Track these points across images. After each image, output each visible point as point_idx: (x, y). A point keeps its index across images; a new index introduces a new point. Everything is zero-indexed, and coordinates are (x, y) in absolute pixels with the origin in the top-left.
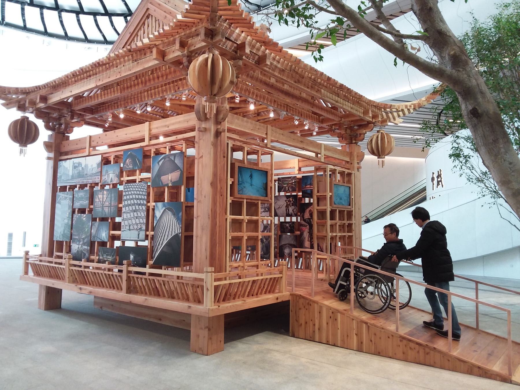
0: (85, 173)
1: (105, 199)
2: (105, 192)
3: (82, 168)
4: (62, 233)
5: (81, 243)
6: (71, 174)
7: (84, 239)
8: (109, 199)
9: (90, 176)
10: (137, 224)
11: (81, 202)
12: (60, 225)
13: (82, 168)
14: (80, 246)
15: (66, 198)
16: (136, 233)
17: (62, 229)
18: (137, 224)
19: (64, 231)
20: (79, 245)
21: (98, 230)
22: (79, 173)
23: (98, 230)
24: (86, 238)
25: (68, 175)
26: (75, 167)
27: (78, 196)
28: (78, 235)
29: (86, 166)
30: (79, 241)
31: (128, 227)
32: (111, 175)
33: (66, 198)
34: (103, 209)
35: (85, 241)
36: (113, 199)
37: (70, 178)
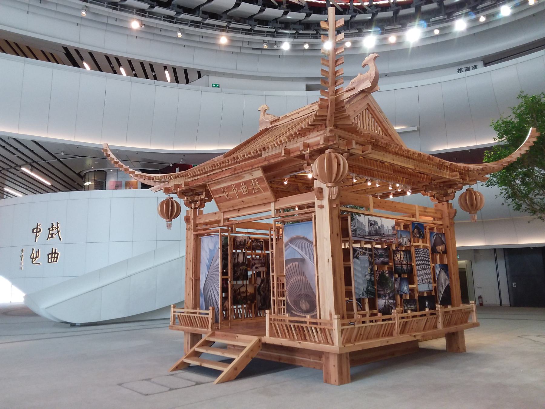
0: (382, 232)
1: (402, 258)
2: (402, 253)
3: (379, 227)
4: (365, 290)
5: (387, 298)
6: (367, 229)
7: (389, 294)
8: (405, 259)
9: (387, 236)
10: (427, 279)
11: (381, 259)
12: (361, 282)
13: (379, 227)
14: (386, 301)
15: (365, 253)
16: (427, 285)
17: (365, 286)
18: (427, 279)
19: (367, 287)
20: (385, 300)
21: (400, 285)
22: (376, 231)
23: (400, 285)
24: (391, 292)
25: (365, 230)
26: (371, 224)
27: (378, 253)
28: (383, 290)
29: (382, 226)
30: (385, 296)
31: (421, 282)
32: (405, 239)
33: (365, 253)
34: (402, 267)
35: (391, 295)
36: (408, 259)
37: (367, 234)
